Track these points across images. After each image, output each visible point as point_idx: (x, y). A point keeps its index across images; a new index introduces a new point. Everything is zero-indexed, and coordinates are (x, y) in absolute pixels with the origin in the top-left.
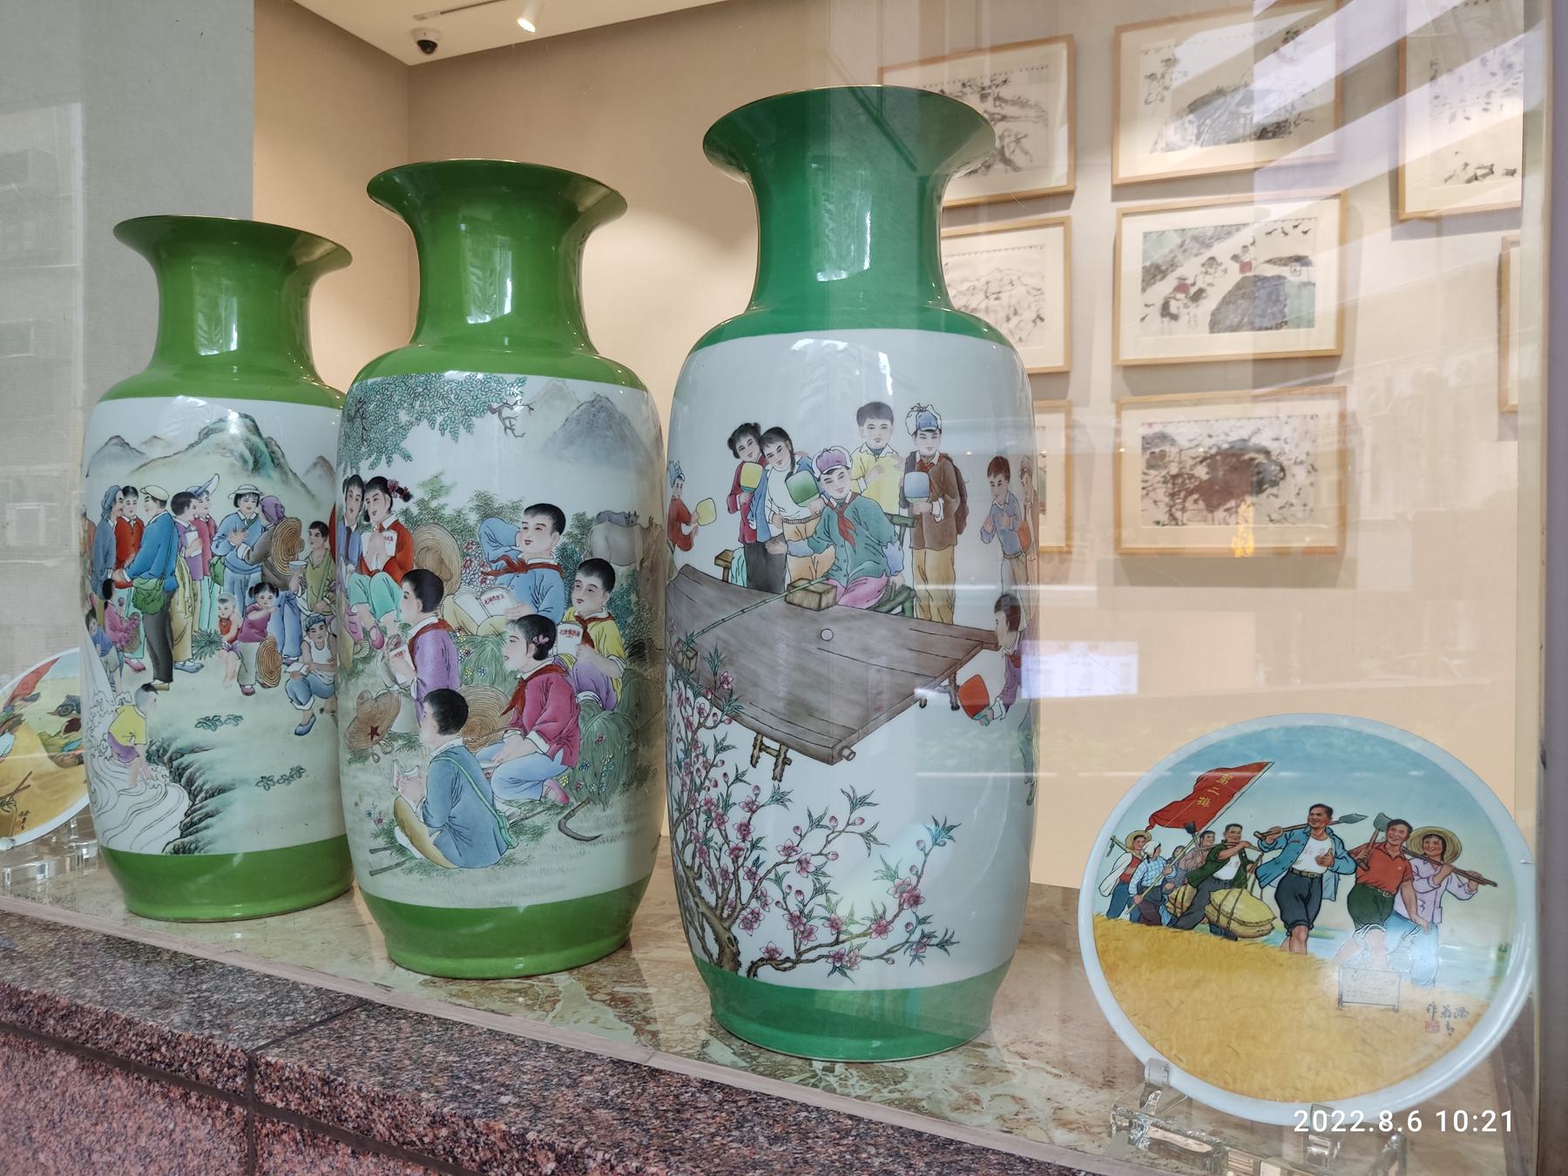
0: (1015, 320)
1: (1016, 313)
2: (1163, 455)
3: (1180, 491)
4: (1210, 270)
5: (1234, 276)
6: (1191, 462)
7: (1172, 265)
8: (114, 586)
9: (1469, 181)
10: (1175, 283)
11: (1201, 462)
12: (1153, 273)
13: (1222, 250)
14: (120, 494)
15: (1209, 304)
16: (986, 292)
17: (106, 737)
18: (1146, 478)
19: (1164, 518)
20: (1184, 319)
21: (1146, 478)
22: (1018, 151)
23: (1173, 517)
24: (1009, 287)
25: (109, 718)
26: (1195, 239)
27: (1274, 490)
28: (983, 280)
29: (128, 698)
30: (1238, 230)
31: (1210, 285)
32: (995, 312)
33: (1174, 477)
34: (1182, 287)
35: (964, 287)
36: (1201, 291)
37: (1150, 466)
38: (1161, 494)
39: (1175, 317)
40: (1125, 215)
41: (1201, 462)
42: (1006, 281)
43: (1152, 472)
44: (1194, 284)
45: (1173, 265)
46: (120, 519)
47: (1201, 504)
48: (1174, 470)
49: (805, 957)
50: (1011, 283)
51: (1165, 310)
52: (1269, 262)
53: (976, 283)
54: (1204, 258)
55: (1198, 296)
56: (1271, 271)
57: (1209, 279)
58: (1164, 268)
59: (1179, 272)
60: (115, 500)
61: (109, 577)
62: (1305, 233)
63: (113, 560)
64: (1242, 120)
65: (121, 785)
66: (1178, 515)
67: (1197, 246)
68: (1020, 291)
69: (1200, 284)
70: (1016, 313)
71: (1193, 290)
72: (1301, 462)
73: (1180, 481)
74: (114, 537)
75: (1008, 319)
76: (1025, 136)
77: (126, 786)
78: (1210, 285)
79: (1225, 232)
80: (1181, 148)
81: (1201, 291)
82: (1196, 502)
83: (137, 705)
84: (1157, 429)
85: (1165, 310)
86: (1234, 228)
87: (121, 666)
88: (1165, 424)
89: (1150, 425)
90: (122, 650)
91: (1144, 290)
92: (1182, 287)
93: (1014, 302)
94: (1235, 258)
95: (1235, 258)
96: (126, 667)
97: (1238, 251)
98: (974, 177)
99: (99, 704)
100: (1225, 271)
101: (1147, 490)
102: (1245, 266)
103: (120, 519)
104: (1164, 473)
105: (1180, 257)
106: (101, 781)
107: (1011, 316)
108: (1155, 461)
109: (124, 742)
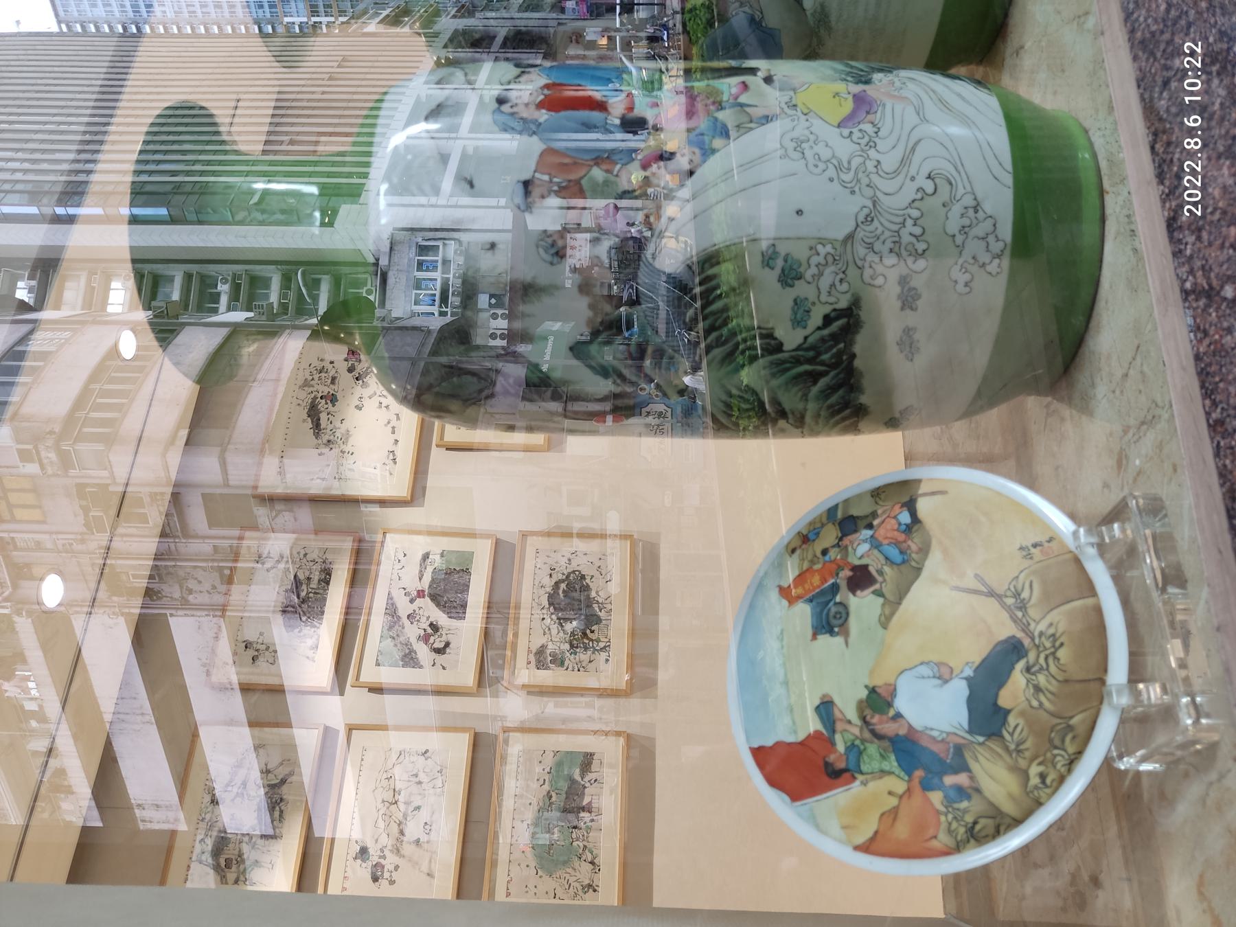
0: (422, 777)
1: (416, 775)
2: (553, 655)
3: (583, 643)
4: (417, 618)
5: (426, 602)
6: (561, 634)
7: (407, 645)
8: (631, 115)
9: (395, 463)
10: (421, 644)
11: (562, 626)
12: (409, 659)
13: (404, 608)
14: (506, 108)
15: (441, 618)
16: (391, 804)
17: (846, 132)
18: (570, 668)
19: (604, 655)
20: (450, 638)
21: (570, 668)
22: (275, 772)
23: (604, 649)
24: (392, 781)
25: (817, 123)
26: (390, 628)
27: (588, 578)
28: (380, 806)
29: (786, 99)
30: (392, 599)
31: (428, 618)
32: (411, 794)
33: (572, 646)
34: (425, 638)
35: (381, 824)
36: (431, 625)
37: (562, 664)
38: (584, 657)
39: (447, 644)
40: (358, 678)
41: (562, 626)
42: (385, 783)
43: (566, 664)
44: (425, 630)
45: (407, 644)
46: (540, 105)
47: (595, 628)
48: (567, 646)
49: (969, 189)
50: (388, 779)
51: (439, 651)
52: (420, 579)
53: (381, 812)
54: (406, 622)
55: (435, 627)
56: (427, 578)
57: (423, 619)
58: (407, 651)
59: (413, 640)
60: (512, 114)
61: (617, 122)
62: (405, 555)
63: (596, 116)
64: (311, 595)
65: (911, 118)
66: (602, 645)
67: (397, 627)
68: (398, 772)
69: (426, 626)
70: (416, 775)
71: (429, 631)
72: (569, 560)
73: (575, 642)
74: (563, 114)
75: (420, 783)
76: (266, 765)
77: (910, 111)
78: (428, 618)
79: (392, 611)
80: (318, 640)
81: (431, 625)
82: (592, 632)
83: (794, 90)
84: (532, 658)
85: (439, 651)
86: (390, 601)
87: (742, 105)
88: (529, 651)
89: (529, 663)
90: (720, 103)
91: (421, 667)
92: (425, 638)
93: (405, 777)
94: (412, 601)
95: (412, 601)
96: (743, 99)
97: (408, 599)
98: (286, 815)
99: (799, 144)
100: (420, 608)
101: (581, 668)
102: (421, 594)
103: (540, 105)
104: (568, 654)
105: (402, 639)
106: (913, 150)
107: (417, 780)
108: (559, 661)
109: (849, 106)
